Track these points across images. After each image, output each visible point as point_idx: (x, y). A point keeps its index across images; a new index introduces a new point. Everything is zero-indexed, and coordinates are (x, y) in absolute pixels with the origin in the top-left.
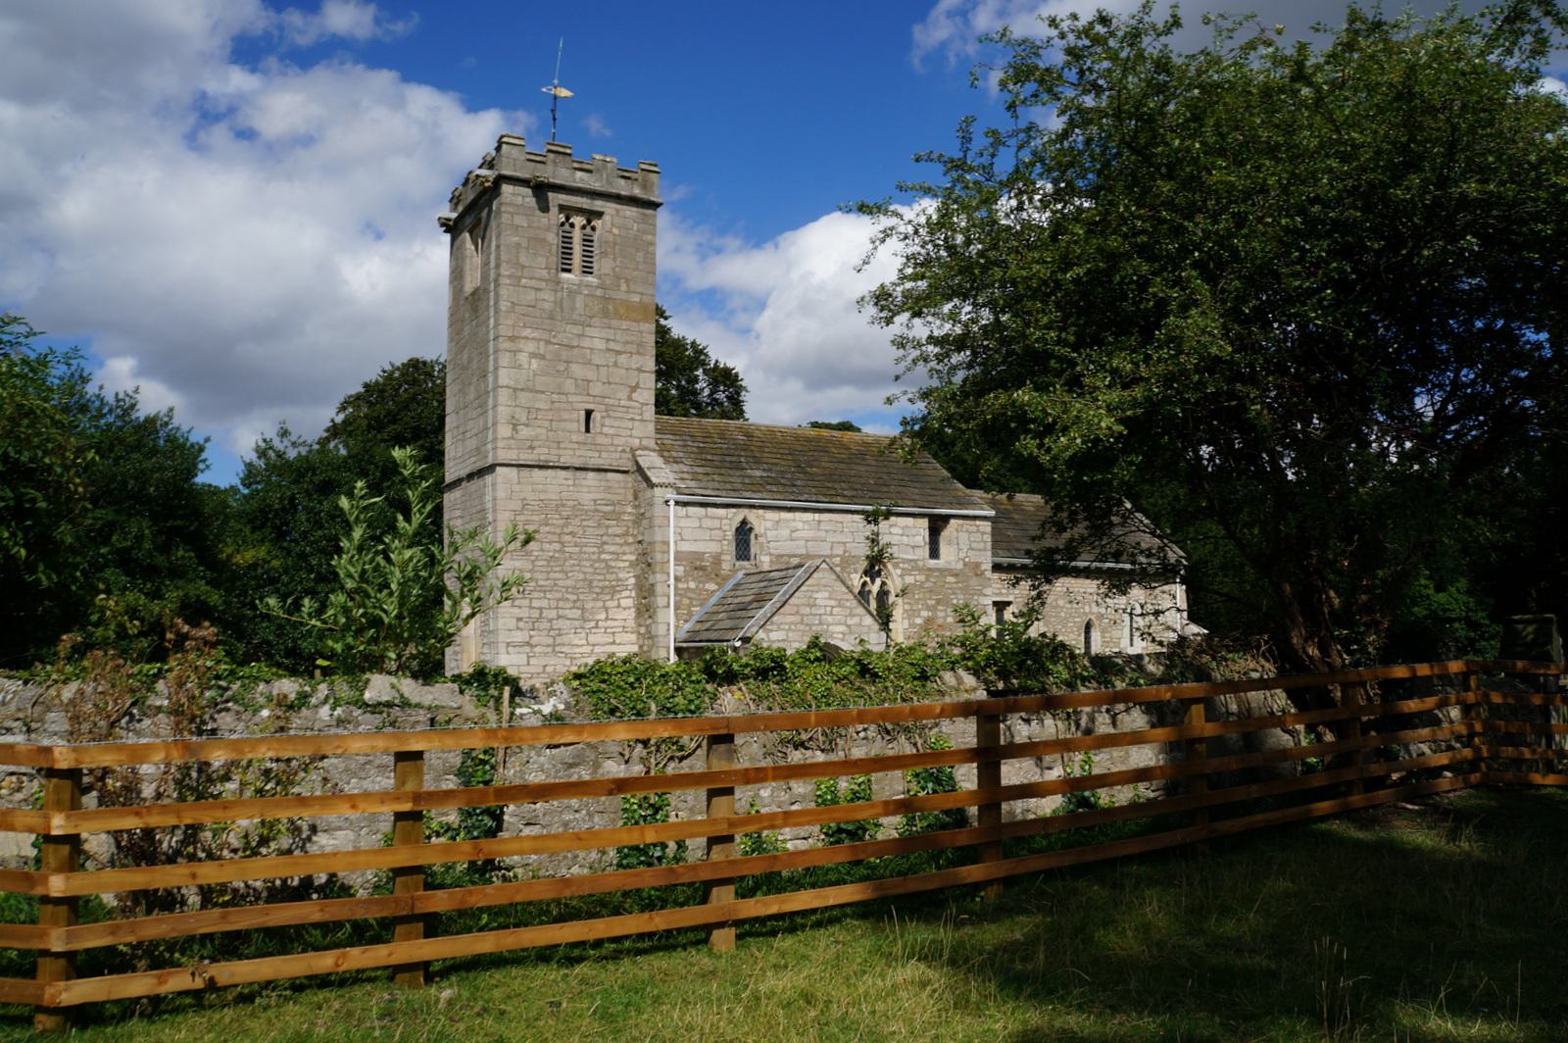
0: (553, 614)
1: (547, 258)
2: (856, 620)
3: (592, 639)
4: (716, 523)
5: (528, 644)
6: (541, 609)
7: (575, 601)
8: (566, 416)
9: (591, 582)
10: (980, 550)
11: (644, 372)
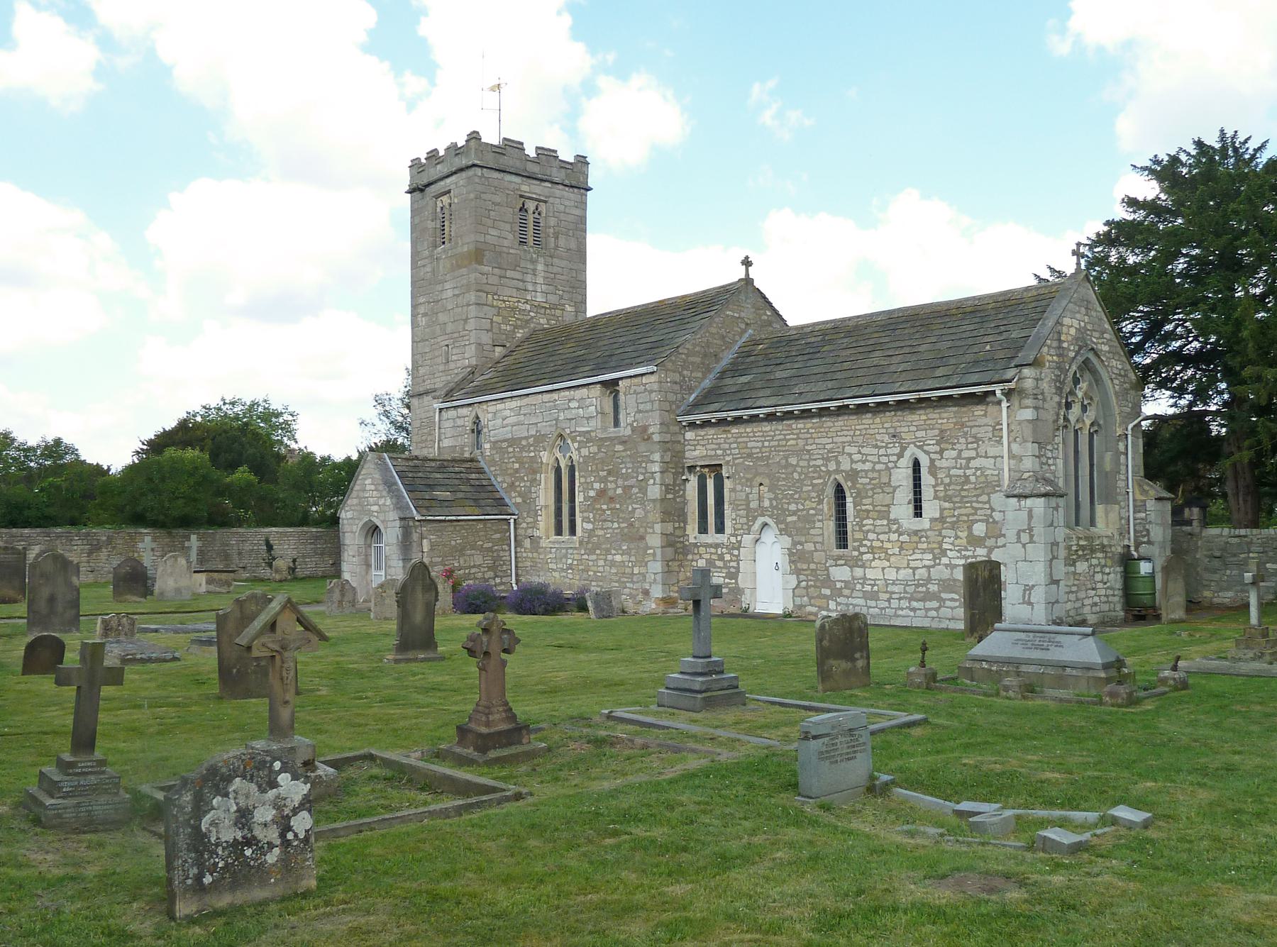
10: (647, 412)
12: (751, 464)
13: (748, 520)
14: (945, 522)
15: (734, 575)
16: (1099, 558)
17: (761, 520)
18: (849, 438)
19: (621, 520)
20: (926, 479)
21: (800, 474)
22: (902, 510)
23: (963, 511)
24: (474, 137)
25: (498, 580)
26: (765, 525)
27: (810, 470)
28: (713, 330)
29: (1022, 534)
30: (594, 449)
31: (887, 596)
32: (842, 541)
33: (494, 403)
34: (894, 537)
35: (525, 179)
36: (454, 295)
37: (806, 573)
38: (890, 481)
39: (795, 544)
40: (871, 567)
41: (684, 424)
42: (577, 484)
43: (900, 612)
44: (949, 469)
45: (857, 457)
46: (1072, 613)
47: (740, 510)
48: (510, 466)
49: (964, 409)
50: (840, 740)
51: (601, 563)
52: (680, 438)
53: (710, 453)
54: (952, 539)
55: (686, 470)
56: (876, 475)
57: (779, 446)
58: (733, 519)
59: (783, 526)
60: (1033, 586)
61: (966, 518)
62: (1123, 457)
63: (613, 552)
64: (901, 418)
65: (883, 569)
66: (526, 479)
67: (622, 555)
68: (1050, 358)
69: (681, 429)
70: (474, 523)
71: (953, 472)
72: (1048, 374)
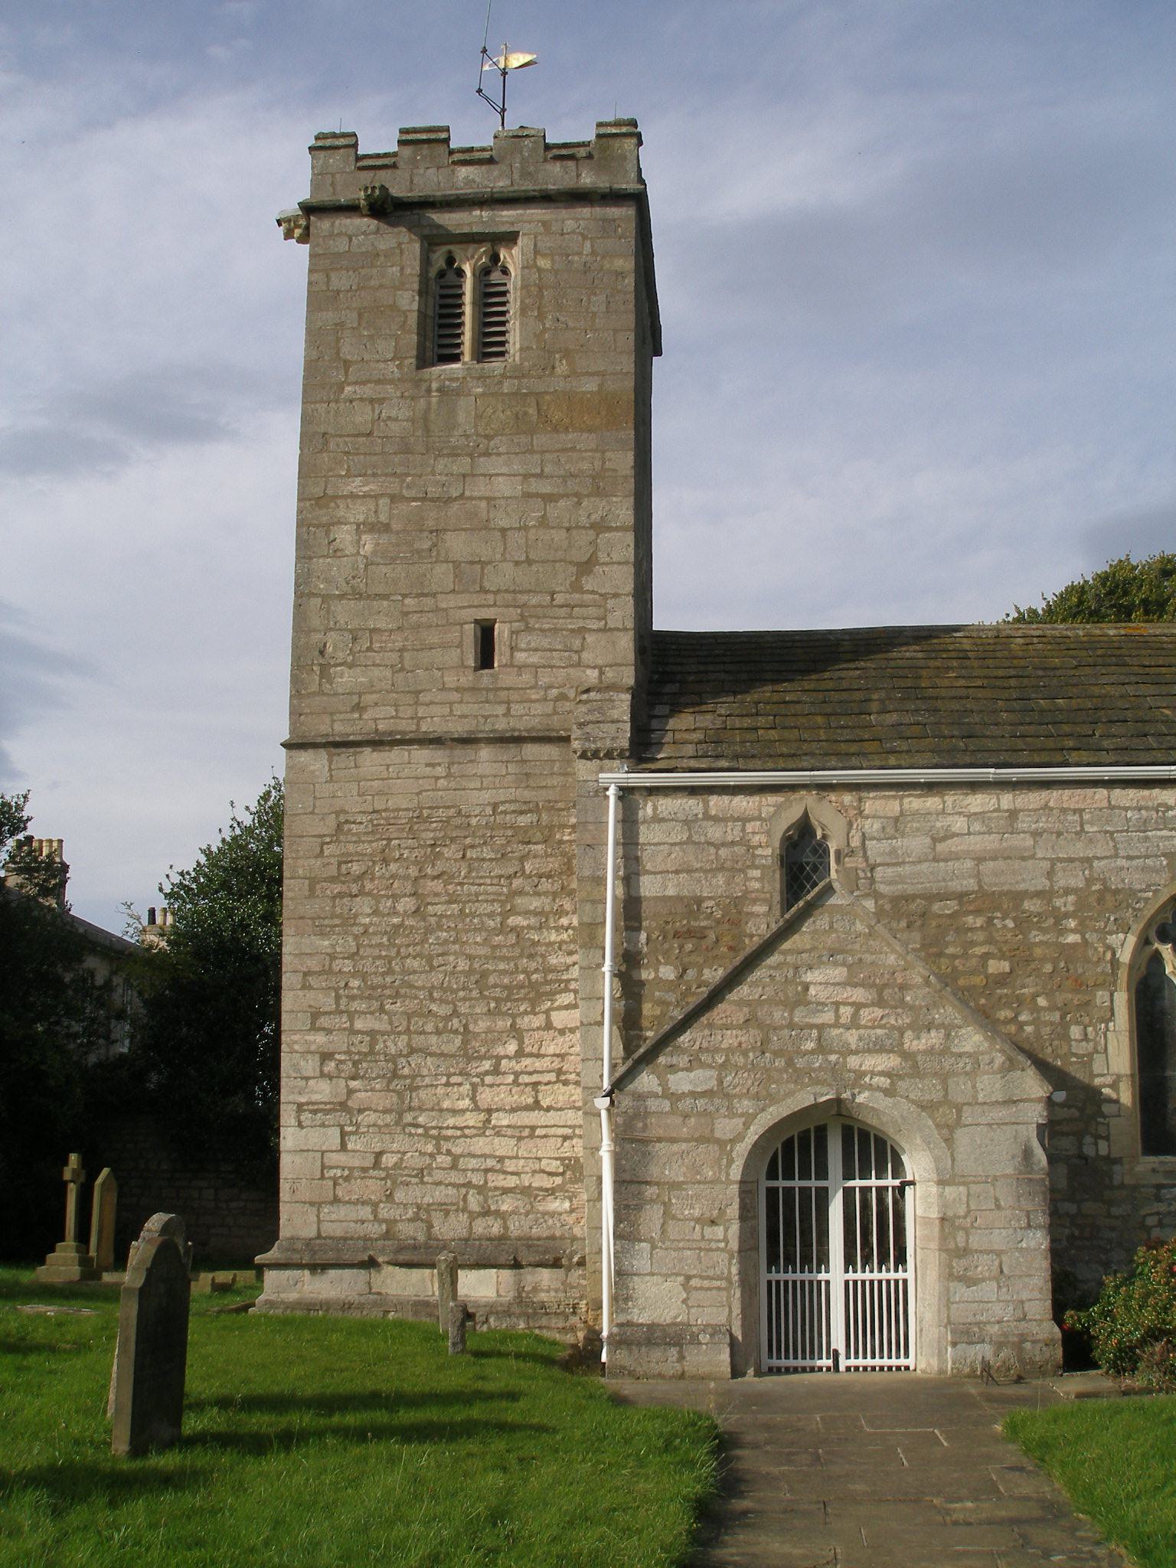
0: (396, 1045)
1: (397, 338)
3: (486, 1097)
4: (733, 832)
5: (343, 1106)
6: (372, 1034)
7: (448, 1018)
8: (434, 638)
9: (484, 975)
11: (610, 529)
66: (1042, 1002)
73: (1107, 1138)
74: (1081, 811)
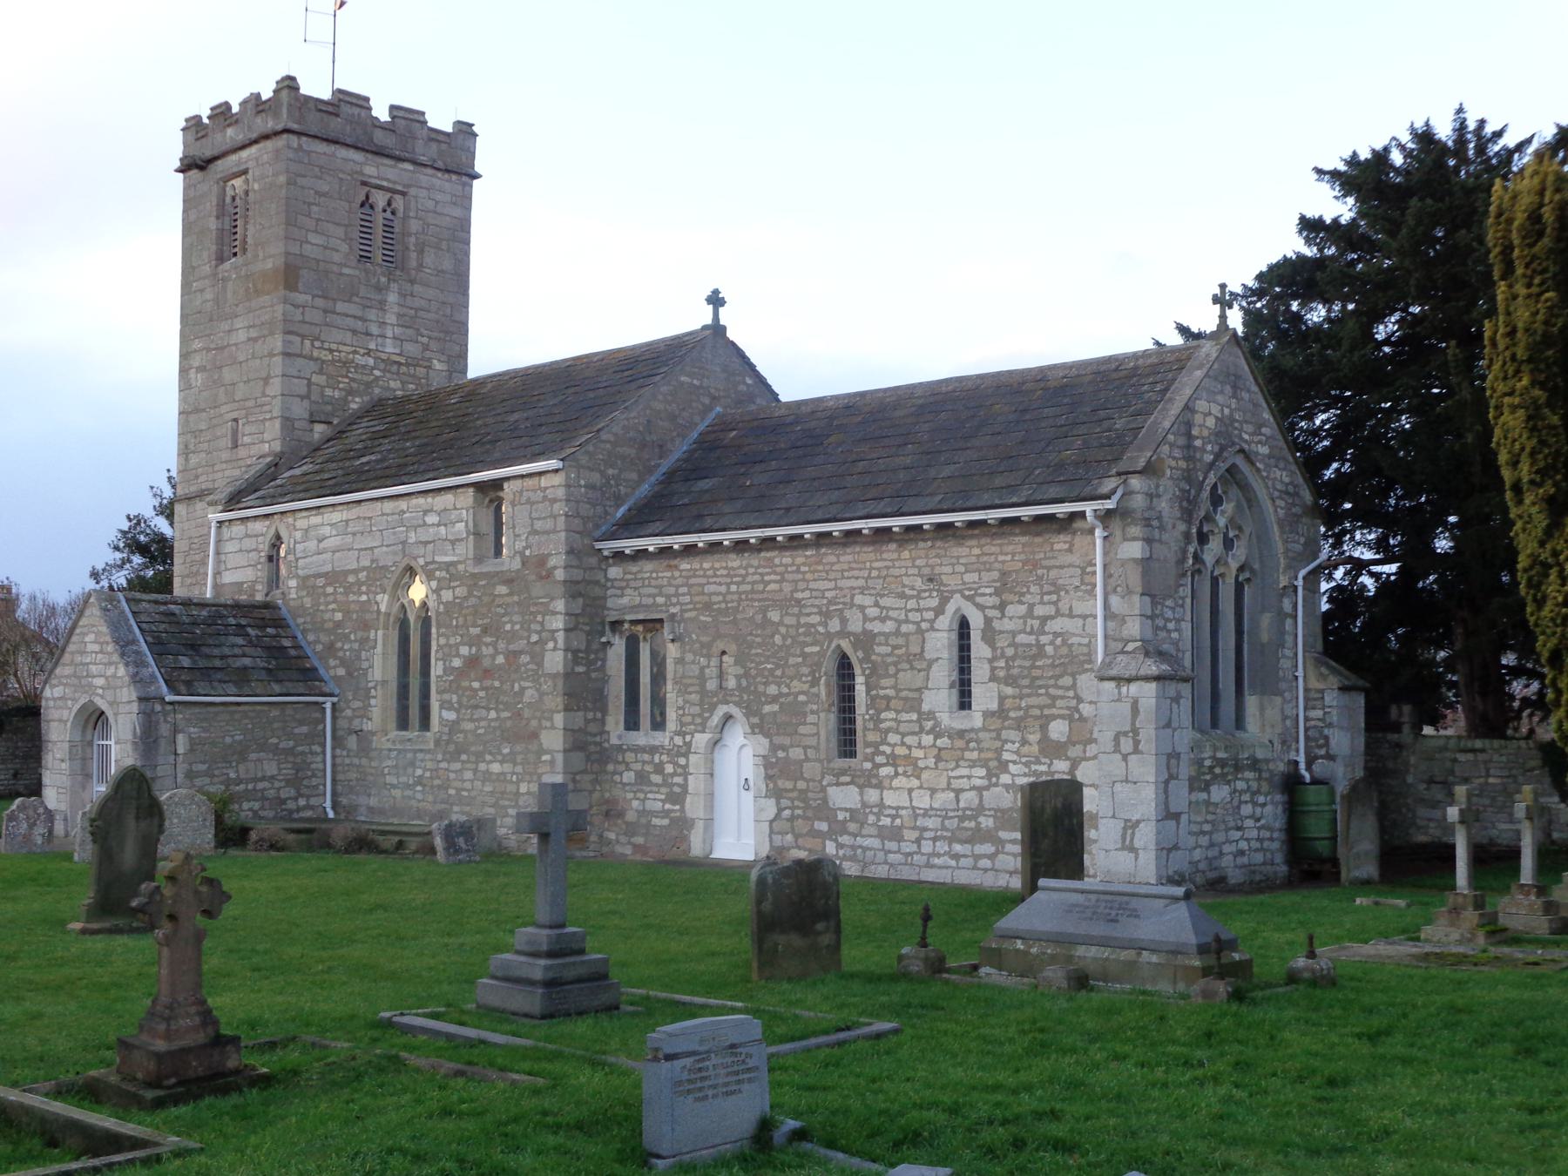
2: (110, 671)
10: (547, 532)
12: (709, 619)
13: (703, 710)
14: (1007, 718)
15: (678, 798)
16: (1247, 781)
17: (722, 710)
18: (861, 582)
19: (501, 706)
20: (979, 649)
21: (784, 638)
22: (939, 698)
23: (1033, 701)
24: (289, 84)
25: (302, 802)
26: (728, 718)
27: (801, 630)
28: (658, 406)
29: (1123, 740)
30: (461, 591)
31: (916, 834)
32: (847, 742)
33: (304, 514)
34: (927, 740)
35: (370, 156)
36: (249, 339)
37: (790, 795)
38: (923, 651)
39: (774, 748)
40: (891, 788)
41: (606, 553)
42: (434, 648)
43: (936, 861)
44: (1014, 634)
45: (873, 612)
46: (1202, 866)
47: (690, 693)
48: (327, 616)
49: (1038, 540)
50: (714, 1062)
51: (468, 775)
52: (600, 577)
53: (646, 601)
54: (1017, 745)
55: (607, 628)
56: (901, 641)
57: (753, 591)
58: (679, 708)
59: (756, 720)
60: (1138, 822)
61: (1037, 712)
62: (1289, 621)
63: (488, 757)
64: (942, 552)
65: (910, 791)
67: (502, 762)
68: (1173, 463)
69: (600, 561)
70: (266, 708)
71: (1021, 638)
72: (1168, 486)
73: (370, 719)
74: (370, 518)
